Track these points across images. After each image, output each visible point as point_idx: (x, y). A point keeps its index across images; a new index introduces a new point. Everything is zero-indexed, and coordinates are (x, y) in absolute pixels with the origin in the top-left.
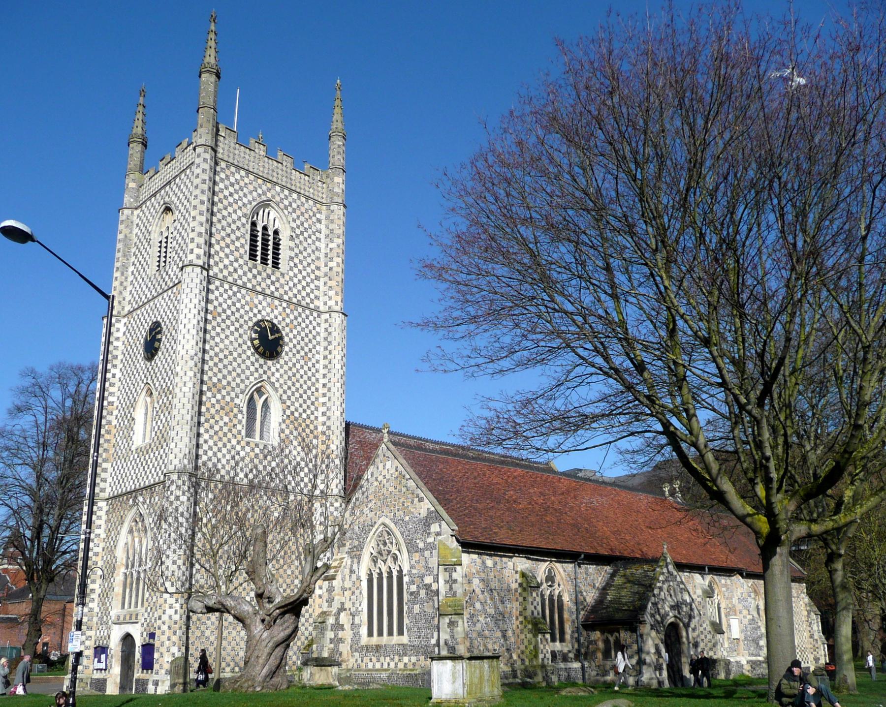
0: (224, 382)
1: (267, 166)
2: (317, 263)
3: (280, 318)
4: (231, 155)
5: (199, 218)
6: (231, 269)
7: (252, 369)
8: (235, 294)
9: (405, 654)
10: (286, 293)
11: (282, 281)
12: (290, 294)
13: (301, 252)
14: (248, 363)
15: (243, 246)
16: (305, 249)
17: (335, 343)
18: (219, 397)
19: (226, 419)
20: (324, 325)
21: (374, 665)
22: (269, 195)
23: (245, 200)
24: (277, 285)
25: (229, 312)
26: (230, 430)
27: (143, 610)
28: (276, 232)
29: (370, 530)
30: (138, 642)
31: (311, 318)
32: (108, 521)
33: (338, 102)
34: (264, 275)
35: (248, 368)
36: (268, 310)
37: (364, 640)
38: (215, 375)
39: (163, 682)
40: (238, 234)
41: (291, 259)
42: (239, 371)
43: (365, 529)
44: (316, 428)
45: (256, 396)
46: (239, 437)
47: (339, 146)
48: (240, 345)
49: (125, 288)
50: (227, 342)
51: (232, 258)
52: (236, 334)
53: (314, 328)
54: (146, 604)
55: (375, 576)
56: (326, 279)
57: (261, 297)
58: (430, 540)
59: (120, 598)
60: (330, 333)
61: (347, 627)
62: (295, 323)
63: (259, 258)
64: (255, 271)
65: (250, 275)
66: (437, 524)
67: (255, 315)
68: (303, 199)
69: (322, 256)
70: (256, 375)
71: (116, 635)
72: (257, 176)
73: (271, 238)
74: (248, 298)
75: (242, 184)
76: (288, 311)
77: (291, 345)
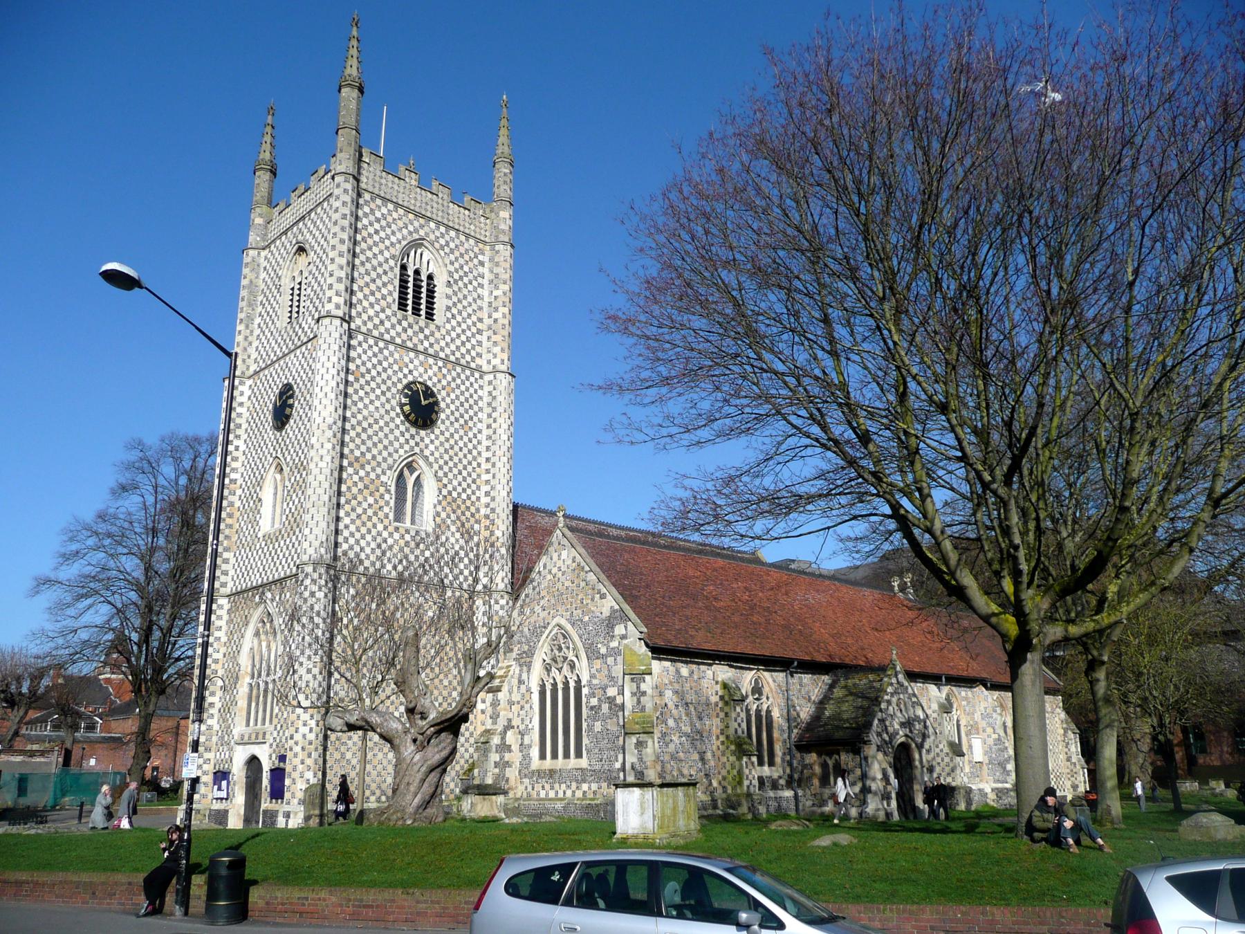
0: (369, 456)
1: (419, 198)
2: (479, 314)
3: (435, 379)
4: (377, 185)
5: (338, 260)
6: (377, 321)
7: (402, 440)
8: (381, 351)
9: (584, 781)
10: (442, 349)
11: (437, 335)
12: (447, 351)
13: (459, 301)
14: (397, 433)
15: (390, 293)
16: (465, 297)
17: (500, 409)
18: (362, 473)
19: (371, 500)
20: (487, 388)
21: (547, 794)
22: (422, 233)
23: (393, 239)
24: (432, 340)
25: (374, 373)
26: (375, 514)
27: (272, 727)
28: (430, 277)
29: (542, 632)
30: (266, 766)
31: (472, 379)
32: (230, 621)
33: (504, 122)
34: (416, 328)
35: (397, 439)
36: (421, 370)
37: (536, 763)
38: (358, 447)
39: (296, 813)
40: (385, 279)
41: (449, 308)
42: (386, 442)
43: (537, 631)
44: (478, 510)
45: (406, 472)
46: (386, 522)
47: (505, 174)
48: (387, 412)
49: (250, 344)
50: (371, 408)
51: (377, 308)
52: (383, 399)
53: (476, 391)
54: (275, 721)
55: (549, 688)
56: (491, 332)
57: (412, 355)
58: (614, 644)
59: (244, 713)
60: (494, 398)
61: (515, 747)
62: (453, 385)
63: (409, 308)
64: (405, 324)
65: (399, 329)
66: (622, 626)
67: (405, 376)
68: (463, 238)
69: (485, 305)
70: (407, 447)
71: (240, 757)
72: (408, 210)
73: (424, 284)
74: (397, 356)
75: (390, 219)
76: (444, 371)
77: (448, 411)
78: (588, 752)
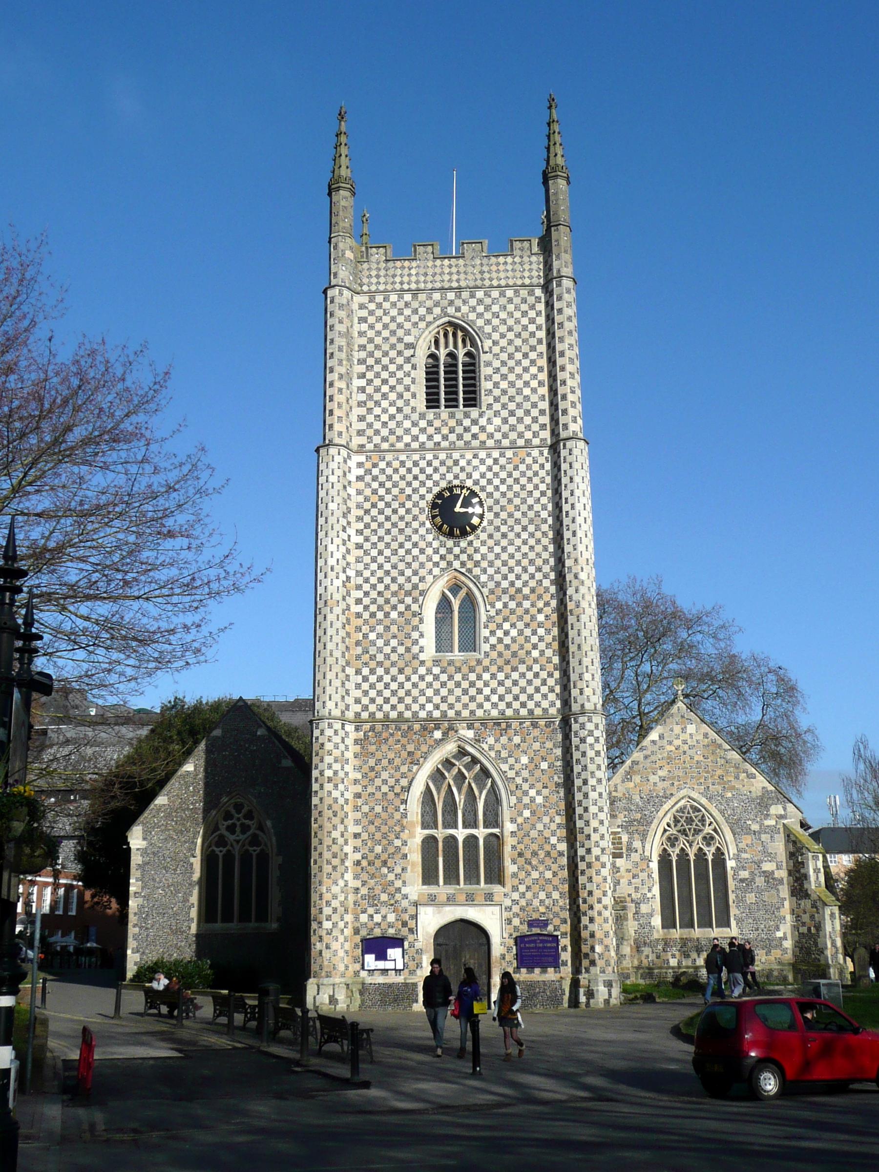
43: (655, 801)
54: (509, 882)
58: (768, 822)
66: (780, 807)
78: (739, 921)
